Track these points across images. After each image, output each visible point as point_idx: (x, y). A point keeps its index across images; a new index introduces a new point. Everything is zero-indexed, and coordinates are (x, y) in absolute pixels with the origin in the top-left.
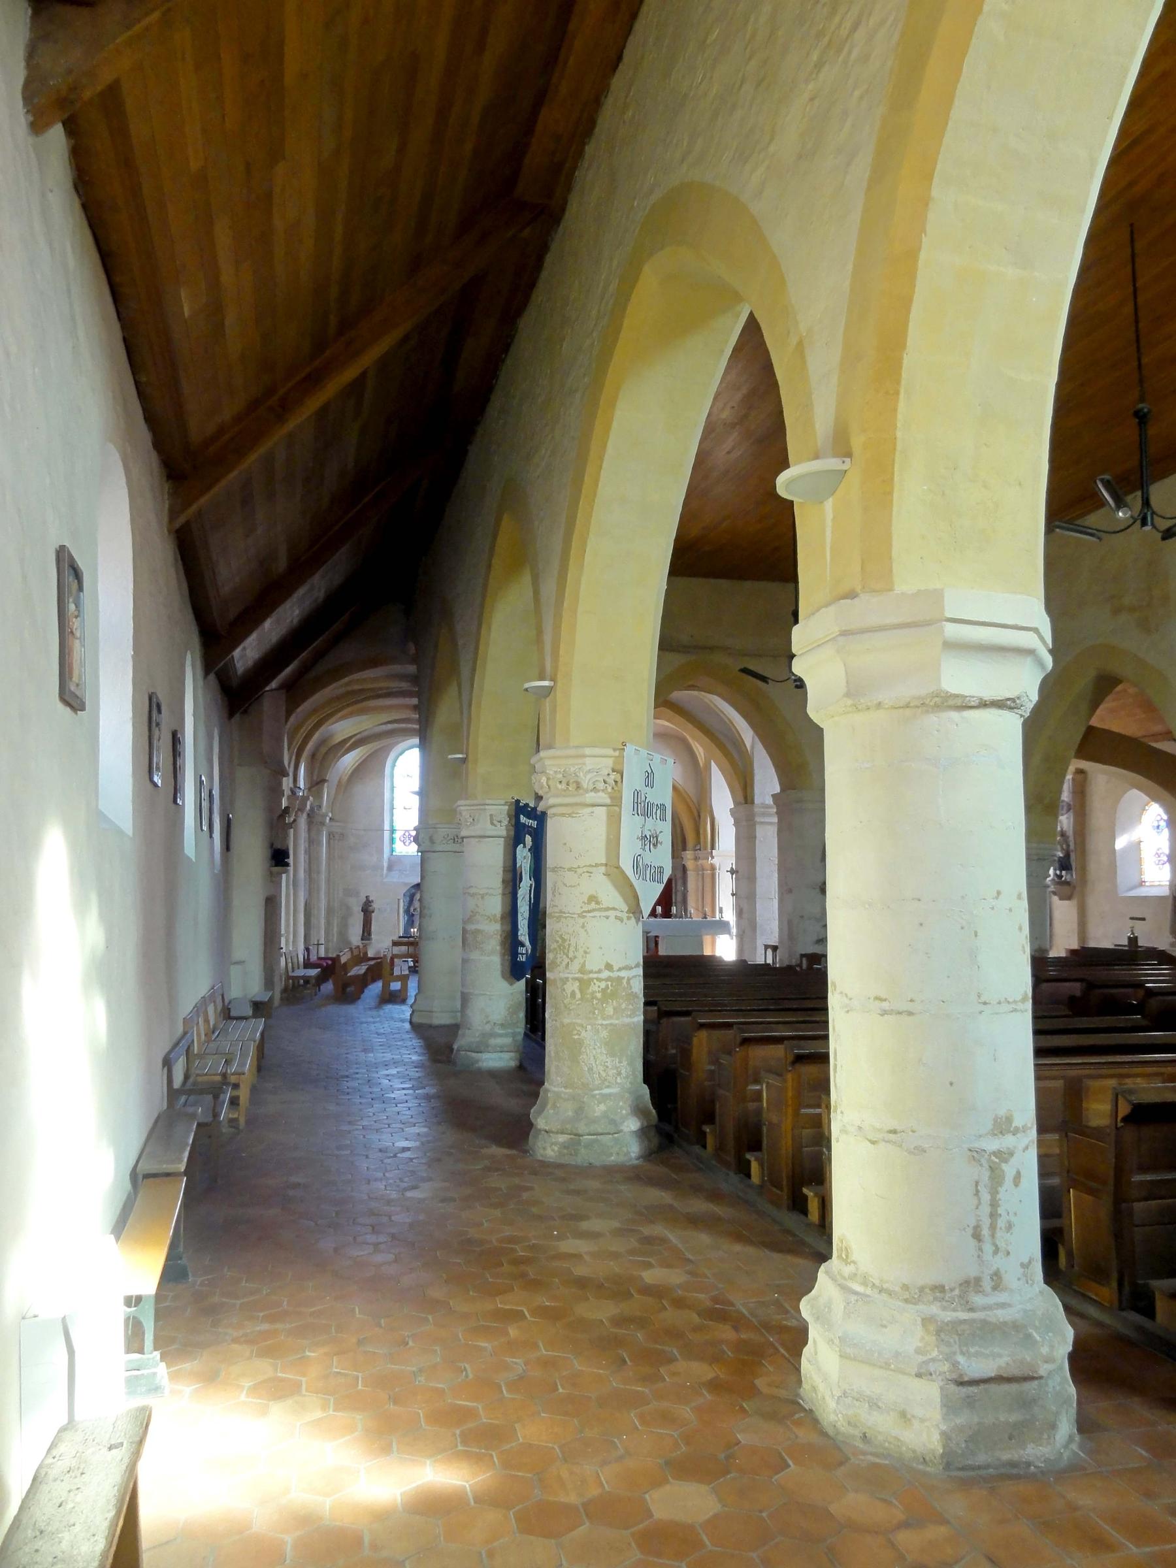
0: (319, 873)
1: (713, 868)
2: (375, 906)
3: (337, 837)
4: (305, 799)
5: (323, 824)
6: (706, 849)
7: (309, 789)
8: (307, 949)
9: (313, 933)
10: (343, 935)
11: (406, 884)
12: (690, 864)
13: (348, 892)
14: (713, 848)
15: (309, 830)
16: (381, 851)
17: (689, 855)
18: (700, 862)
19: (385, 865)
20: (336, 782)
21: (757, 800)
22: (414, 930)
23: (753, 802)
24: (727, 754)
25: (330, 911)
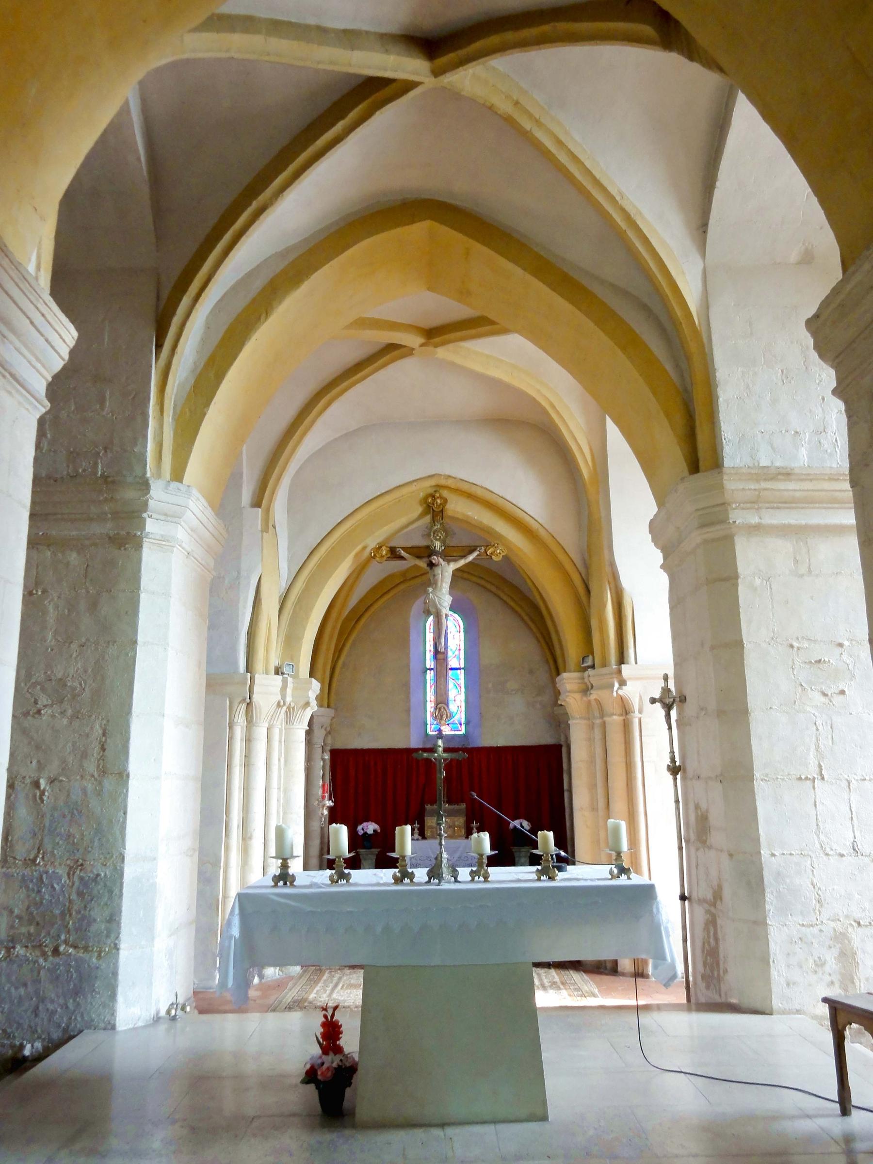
1: (626, 710)
6: (604, 664)
12: (572, 702)
14: (622, 659)
17: (569, 680)
18: (594, 695)
21: (733, 456)
23: (717, 464)
24: (629, 342)
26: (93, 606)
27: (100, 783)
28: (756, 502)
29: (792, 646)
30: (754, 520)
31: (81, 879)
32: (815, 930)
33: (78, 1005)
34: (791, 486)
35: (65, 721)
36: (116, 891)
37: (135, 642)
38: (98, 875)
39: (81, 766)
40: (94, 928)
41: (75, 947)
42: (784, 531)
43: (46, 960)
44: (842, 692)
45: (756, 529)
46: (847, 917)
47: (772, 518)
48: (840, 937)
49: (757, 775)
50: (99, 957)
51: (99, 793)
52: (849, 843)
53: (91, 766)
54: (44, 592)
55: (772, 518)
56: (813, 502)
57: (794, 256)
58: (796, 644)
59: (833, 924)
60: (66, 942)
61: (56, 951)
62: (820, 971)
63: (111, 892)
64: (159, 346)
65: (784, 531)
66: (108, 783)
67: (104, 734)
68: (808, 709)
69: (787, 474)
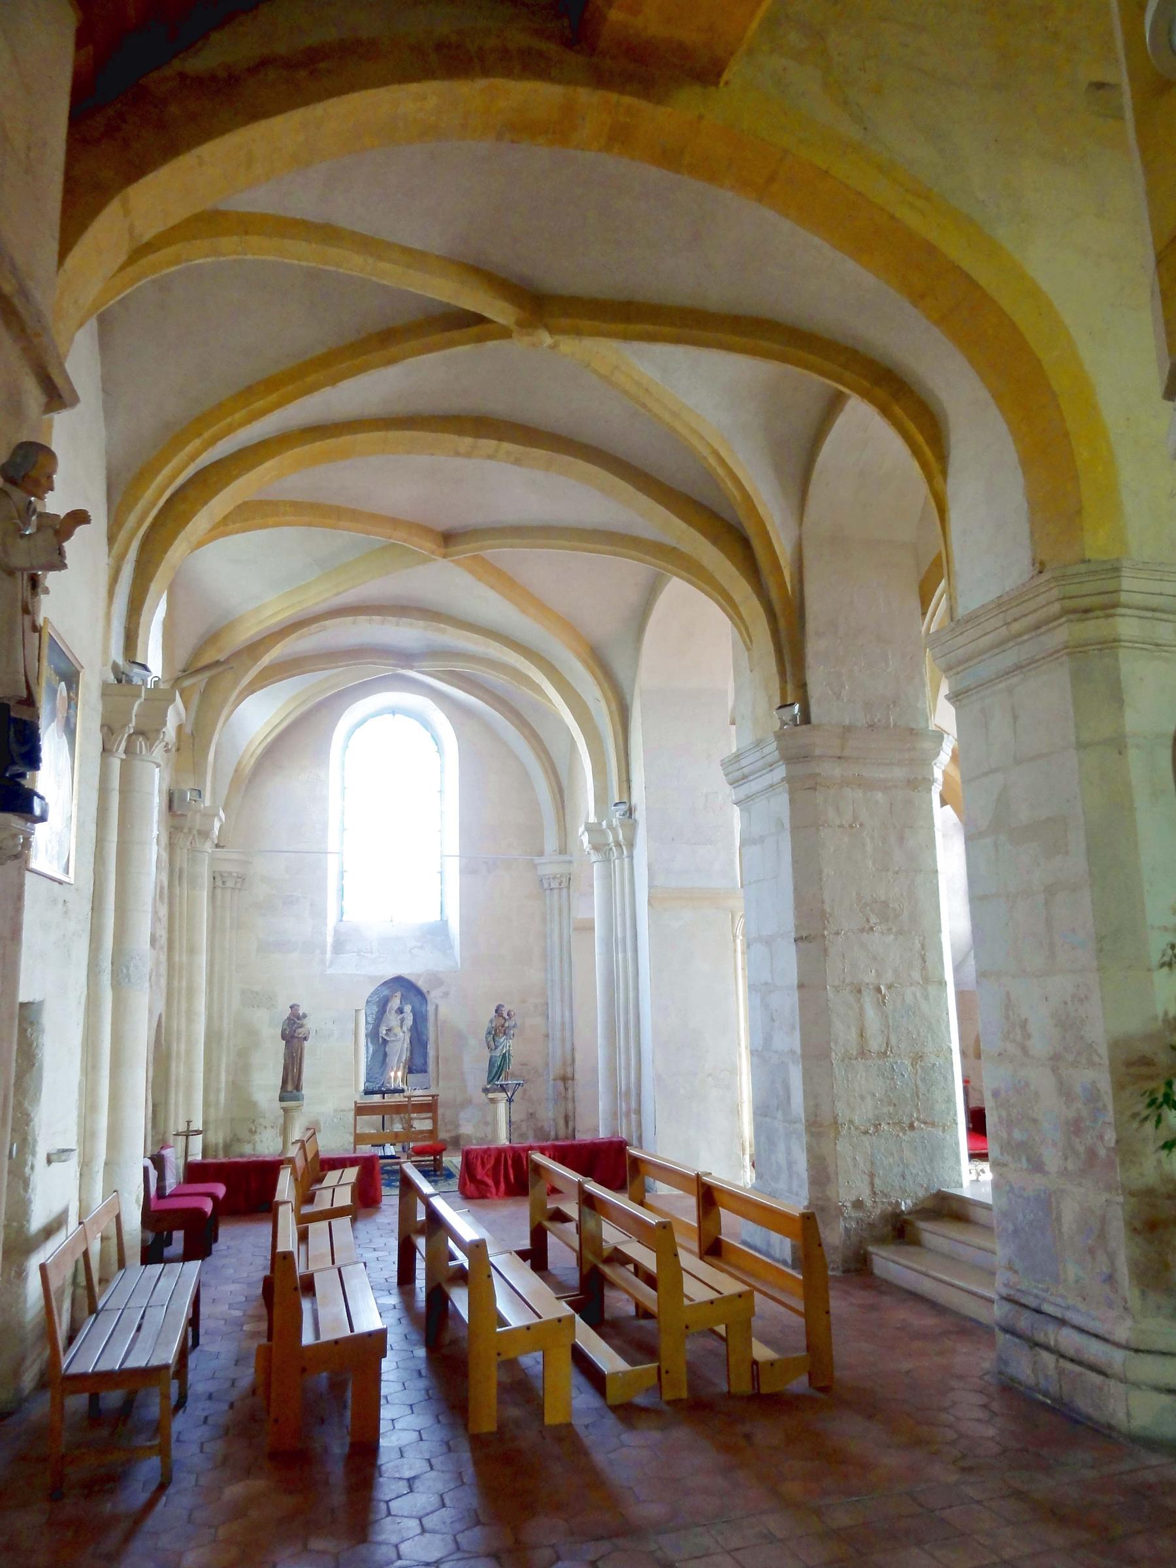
0: (192, 951)
2: (310, 1024)
3: (230, 884)
4: (158, 700)
5: (205, 834)
7: (177, 681)
8: (158, 1161)
9: (176, 1098)
10: (239, 1090)
11: (372, 979)
13: (255, 999)
15: (171, 847)
16: (319, 913)
19: (330, 940)
20: (232, 769)
22: (396, 1076)
25: (213, 1037)
26: (901, 839)
27: (926, 989)
31: (922, 1068)
33: (933, 1169)
35: (892, 937)
36: (950, 1077)
37: (937, 871)
38: (934, 1065)
39: (910, 975)
40: (937, 1107)
41: (925, 1123)
43: (904, 1134)
50: (944, 1131)
51: (926, 998)
53: (916, 975)
54: (861, 825)
60: (918, 1119)
61: (911, 1127)
63: (945, 1078)
64: (924, 614)
66: (932, 990)
67: (923, 947)
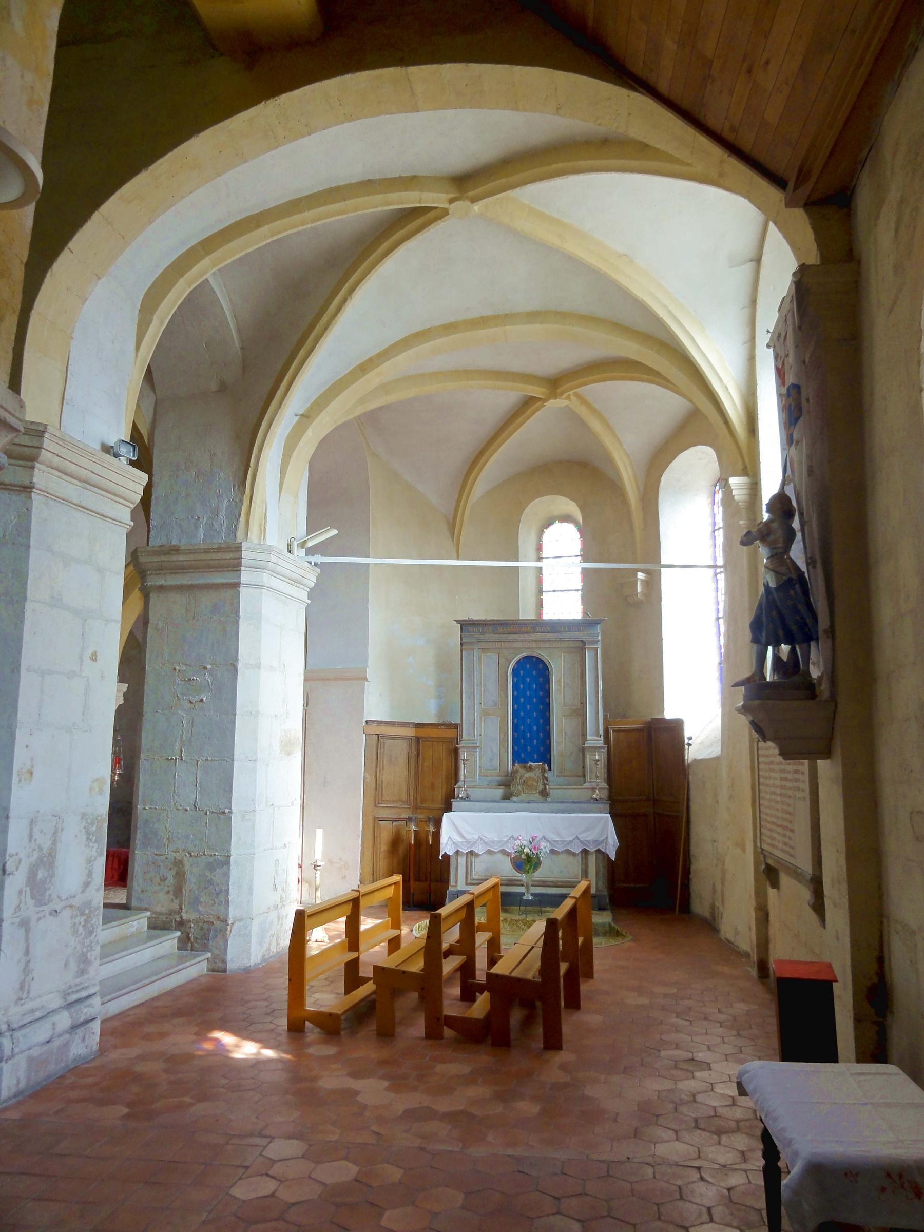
28: (161, 569)
29: (175, 669)
30: (162, 582)
32: (163, 858)
34: (181, 558)
42: (180, 588)
44: (202, 701)
45: (161, 588)
46: (184, 850)
47: (172, 580)
48: (178, 863)
49: (143, 756)
52: (192, 802)
55: (172, 580)
56: (209, 567)
57: (214, 386)
58: (177, 668)
59: (174, 854)
62: (162, 883)
65: (180, 588)
68: (180, 712)
69: (176, 550)
